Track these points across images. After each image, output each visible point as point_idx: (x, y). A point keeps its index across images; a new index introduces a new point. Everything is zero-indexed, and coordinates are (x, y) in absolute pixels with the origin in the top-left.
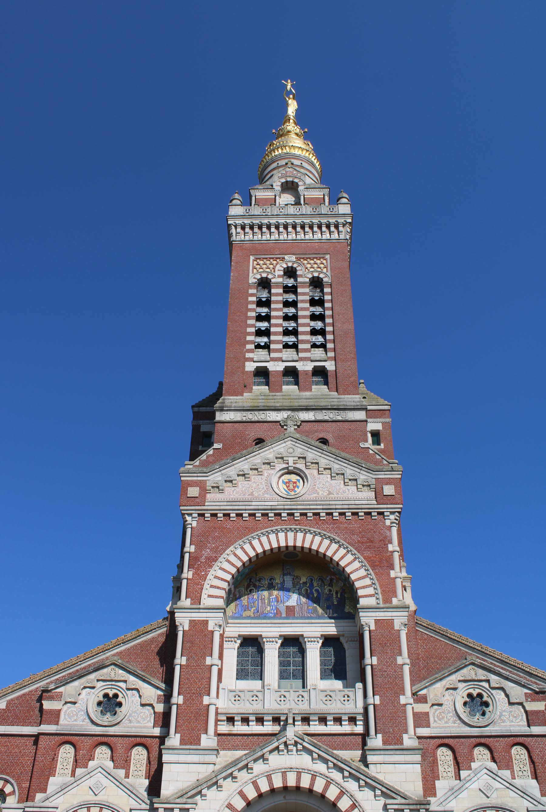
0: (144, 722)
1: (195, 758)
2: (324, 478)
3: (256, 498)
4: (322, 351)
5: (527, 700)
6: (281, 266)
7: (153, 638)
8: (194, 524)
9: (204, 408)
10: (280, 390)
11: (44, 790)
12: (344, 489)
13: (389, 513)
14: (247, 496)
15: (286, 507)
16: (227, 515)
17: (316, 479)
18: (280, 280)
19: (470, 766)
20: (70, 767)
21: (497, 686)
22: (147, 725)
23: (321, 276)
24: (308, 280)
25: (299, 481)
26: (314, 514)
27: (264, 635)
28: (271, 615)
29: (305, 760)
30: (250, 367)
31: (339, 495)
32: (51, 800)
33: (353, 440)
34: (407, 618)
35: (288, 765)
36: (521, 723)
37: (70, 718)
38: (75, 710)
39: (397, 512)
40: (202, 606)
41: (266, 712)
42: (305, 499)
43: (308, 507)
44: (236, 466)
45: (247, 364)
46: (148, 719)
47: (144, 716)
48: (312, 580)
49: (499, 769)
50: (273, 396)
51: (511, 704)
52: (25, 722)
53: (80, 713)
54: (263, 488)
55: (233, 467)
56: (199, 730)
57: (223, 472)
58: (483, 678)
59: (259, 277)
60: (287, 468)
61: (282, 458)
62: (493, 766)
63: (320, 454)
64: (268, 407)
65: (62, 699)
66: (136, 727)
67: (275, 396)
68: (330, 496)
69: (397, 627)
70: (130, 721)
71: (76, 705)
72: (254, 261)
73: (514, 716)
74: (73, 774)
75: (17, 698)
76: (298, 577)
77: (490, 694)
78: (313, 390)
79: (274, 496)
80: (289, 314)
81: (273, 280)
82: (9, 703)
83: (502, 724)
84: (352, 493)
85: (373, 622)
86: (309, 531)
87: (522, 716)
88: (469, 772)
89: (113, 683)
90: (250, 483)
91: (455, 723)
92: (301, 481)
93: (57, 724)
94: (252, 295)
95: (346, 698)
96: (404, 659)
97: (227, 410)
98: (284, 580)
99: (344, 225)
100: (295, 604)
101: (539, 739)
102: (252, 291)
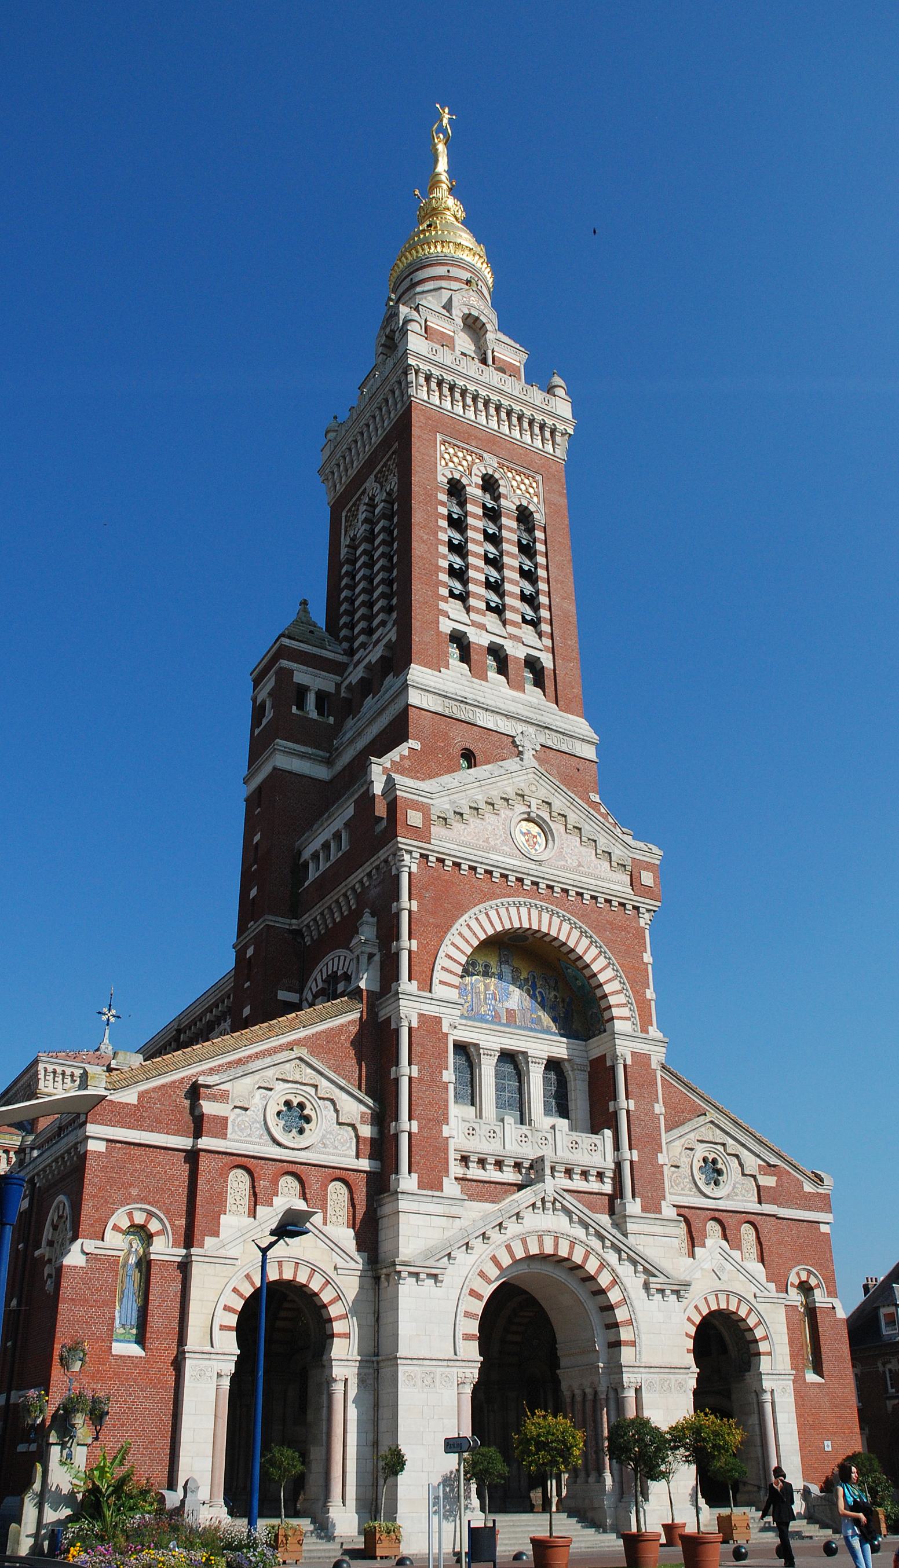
0: (344, 1148)
1: (439, 1209)
8: (414, 869)
11: (216, 1234)
14: (481, 843)
15: (532, 872)
16: (457, 865)
17: (563, 840)
19: (704, 1243)
20: (246, 1201)
21: (733, 1152)
22: (347, 1152)
25: (539, 834)
26: (563, 890)
27: (482, 1044)
28: (488, 1017)
29: (560, 1222)
30: (446, 626)
33: (581, 787)
34: (664, 1055)
35: (544, 1227)
36: (751, 1199)
37: (241, 1130)
38: (247, 1119)
39: (654, 911)
40: (434, 996)
41: (508, 1154)
44: (467, 792)
46: (348, 1145)
47: (342, 1140)
49: (731, 1249)
51: (744, 1174)
52: (170, 1129)
53: (255, 1125)
55: (464, 793)
56: (440, 1172)
57: (452, 797)
58: (720, 1141)
60: (529, 813)
61: (523, 796)
62: (724, 1243)
63: (569, 804)
65: (230, 1101)
68: (580, 868)
69: (654, 1067)
70: (325, 1146)
71: (247, 1112)
73: (745, 1190)
75: (154, 1089)
77: (725, 1161)
82: (141, 1095)
83: (735, 1198)
85: (629, 1054)
86: (558, 913)
87: (753, 1190)
88: (703, 1249)
89: (298, 1086)
90: (484, 823)
91: (691, 1191)
93: (224, 1136)
94: (443, 504)
95: (593, 1147)
96: (659, 1108)
98: (501, 970)
99: (563, 434)
101: (768, 1218)
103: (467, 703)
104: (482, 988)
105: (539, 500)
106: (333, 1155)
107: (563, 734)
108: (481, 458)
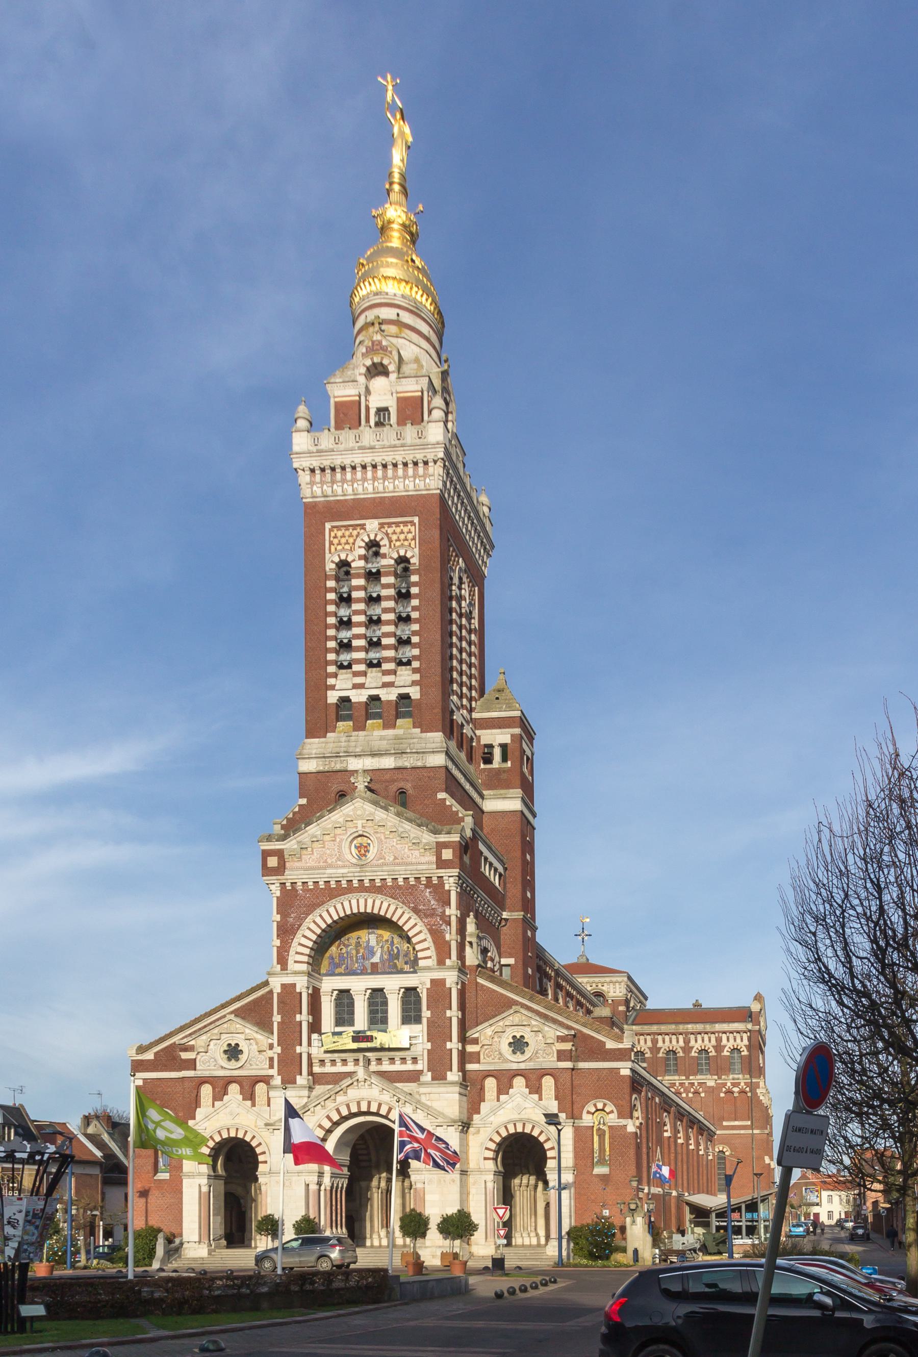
5: (558, 1042)
7: (263, 995)
23: (409, 555)
24: (392, 562)
30: (333, 697)
32: (200, 1124)
37: (204, 1064)
45: (329, 693)
48: (393, 938)
59: (337, 560)
66: (255, 1069)
70: (251, 1065)
72: (330, 530)
74: (213, 1106)
76: (381, 936)
81: (353, 565)
82: (156, 1054)
100: (378, 961)
102: (331, 584)
103: (340, 756)
104: (354, 952)
106: (255, 1069)
107: (417, 753)
108: (363, 527)
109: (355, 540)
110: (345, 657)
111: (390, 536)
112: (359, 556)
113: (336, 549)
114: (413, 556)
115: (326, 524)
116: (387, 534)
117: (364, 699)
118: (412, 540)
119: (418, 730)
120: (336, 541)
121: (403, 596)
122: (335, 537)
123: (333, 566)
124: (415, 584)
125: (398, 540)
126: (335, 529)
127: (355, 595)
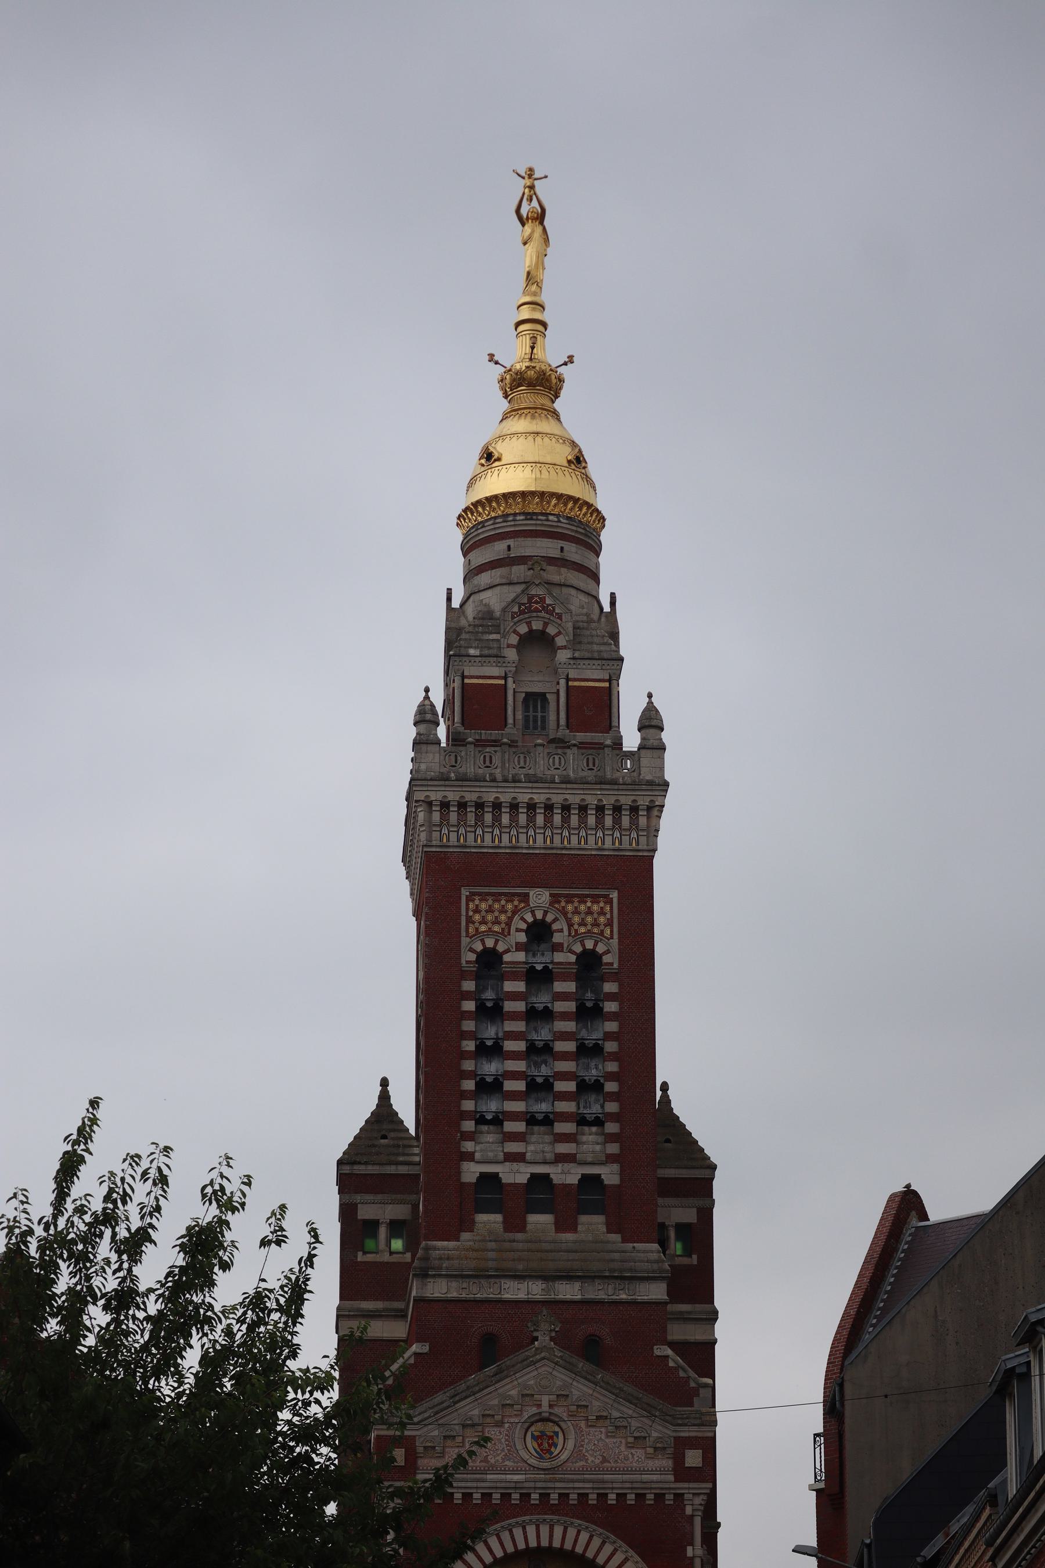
2: (596, 1433)
3: (493, 1466)
4: (596, 1134)
6: (523, 919)
9: (362, 1167)
10: (522, 1227)
12: (626, 1453)
13: (691, 1496)
15: (539, 1485)
17: (583, 1435)
18: (521, 956)
23: (601, 948)
24: (573, 958)
30: (470, 1172)
31: (618, 1464)
42: (566, 1470)
43: (571, 1485)
44: (459, 1412)
50: (510, 1241)
54: (503, 1450)
55: (456, 1413)
59: (479, 947)
60: (540, 1413)
64: (503, 1270)
67: (514, 1241)
68: (605, 1464)
72: (469, 899)
78: (580, 1228)
79: (519, 1464)
80: (537, 1043)
81: (507, 958)
84: (637, 1460)
92: (561, 1435)
97: (434, 1276)
102: (469, 986)
105: (612, 931)
109: (510, 919)
110: (492, 1106)
111: (570, 915)
112: (517, 944)
113: (477, 929)
114: (608, 952)
115: (462, 888)
116: (564, 913)
117: (522, 1179)
118: (605, 925)
119: (616, 1237)
120: (477, 917)
121: (588, 1013)
122: (477, 911)
123: (472, 957)
124: (611, 997)
125: (583, 923)
126: (477, 898)
127: (509, 1006)
